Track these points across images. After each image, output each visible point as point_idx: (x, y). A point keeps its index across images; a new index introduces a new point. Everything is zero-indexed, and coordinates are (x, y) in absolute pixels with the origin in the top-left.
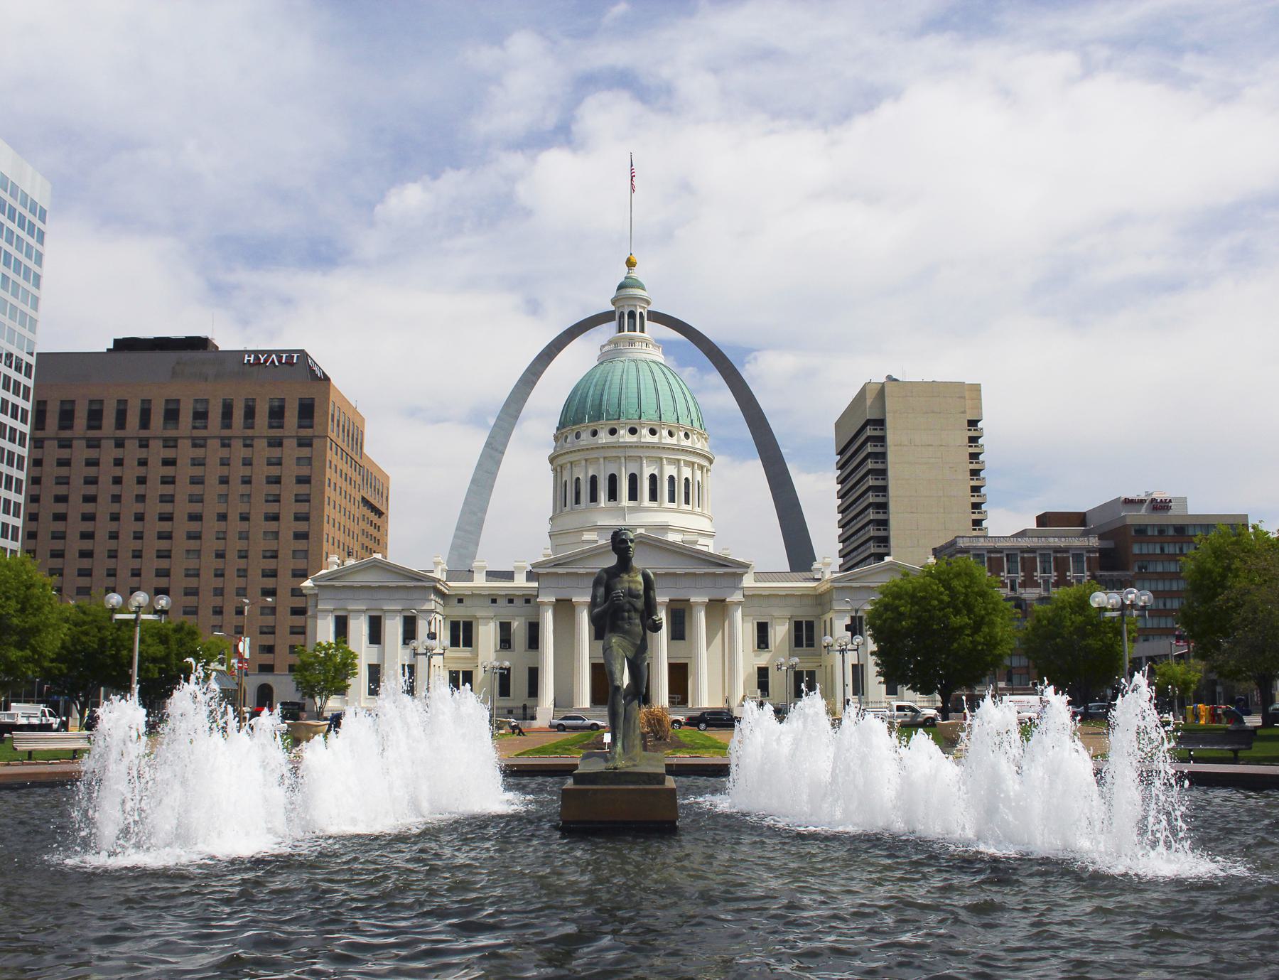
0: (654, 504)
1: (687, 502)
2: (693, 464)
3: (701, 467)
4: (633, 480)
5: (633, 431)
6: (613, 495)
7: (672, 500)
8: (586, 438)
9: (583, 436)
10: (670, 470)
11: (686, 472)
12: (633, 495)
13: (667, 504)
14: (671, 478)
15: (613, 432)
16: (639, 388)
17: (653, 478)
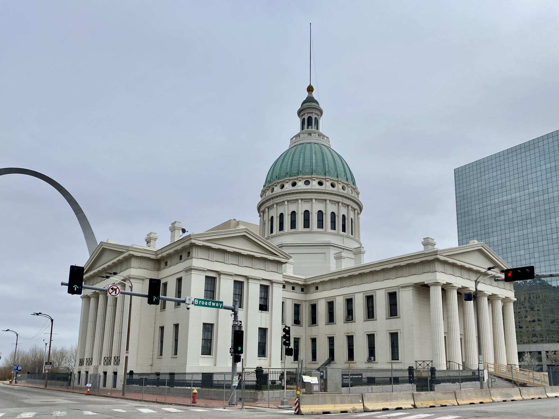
0: (320, 230)
1: (344, 230)
2: (348, 206)
3: (354, 210)
4: (307, 214)
5: (307, 183)
6: (293, 225)
7: (333, 227)
8: (277, 190)
9: (275, 189)
10: (332, 208)
11: (343, 211)
12: (307, 224)
13: (329, 230)
14: (333, 214)
15: (294, 184)
16: (311, 157)
17: (320, 213)
